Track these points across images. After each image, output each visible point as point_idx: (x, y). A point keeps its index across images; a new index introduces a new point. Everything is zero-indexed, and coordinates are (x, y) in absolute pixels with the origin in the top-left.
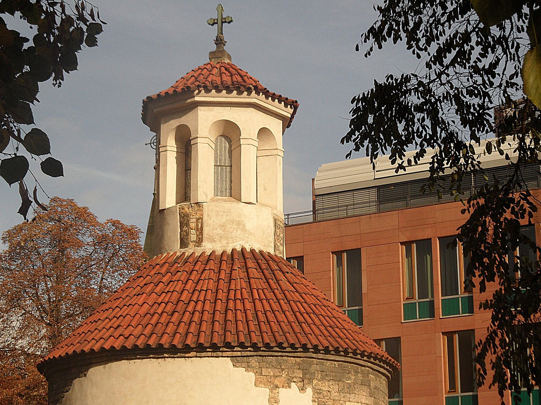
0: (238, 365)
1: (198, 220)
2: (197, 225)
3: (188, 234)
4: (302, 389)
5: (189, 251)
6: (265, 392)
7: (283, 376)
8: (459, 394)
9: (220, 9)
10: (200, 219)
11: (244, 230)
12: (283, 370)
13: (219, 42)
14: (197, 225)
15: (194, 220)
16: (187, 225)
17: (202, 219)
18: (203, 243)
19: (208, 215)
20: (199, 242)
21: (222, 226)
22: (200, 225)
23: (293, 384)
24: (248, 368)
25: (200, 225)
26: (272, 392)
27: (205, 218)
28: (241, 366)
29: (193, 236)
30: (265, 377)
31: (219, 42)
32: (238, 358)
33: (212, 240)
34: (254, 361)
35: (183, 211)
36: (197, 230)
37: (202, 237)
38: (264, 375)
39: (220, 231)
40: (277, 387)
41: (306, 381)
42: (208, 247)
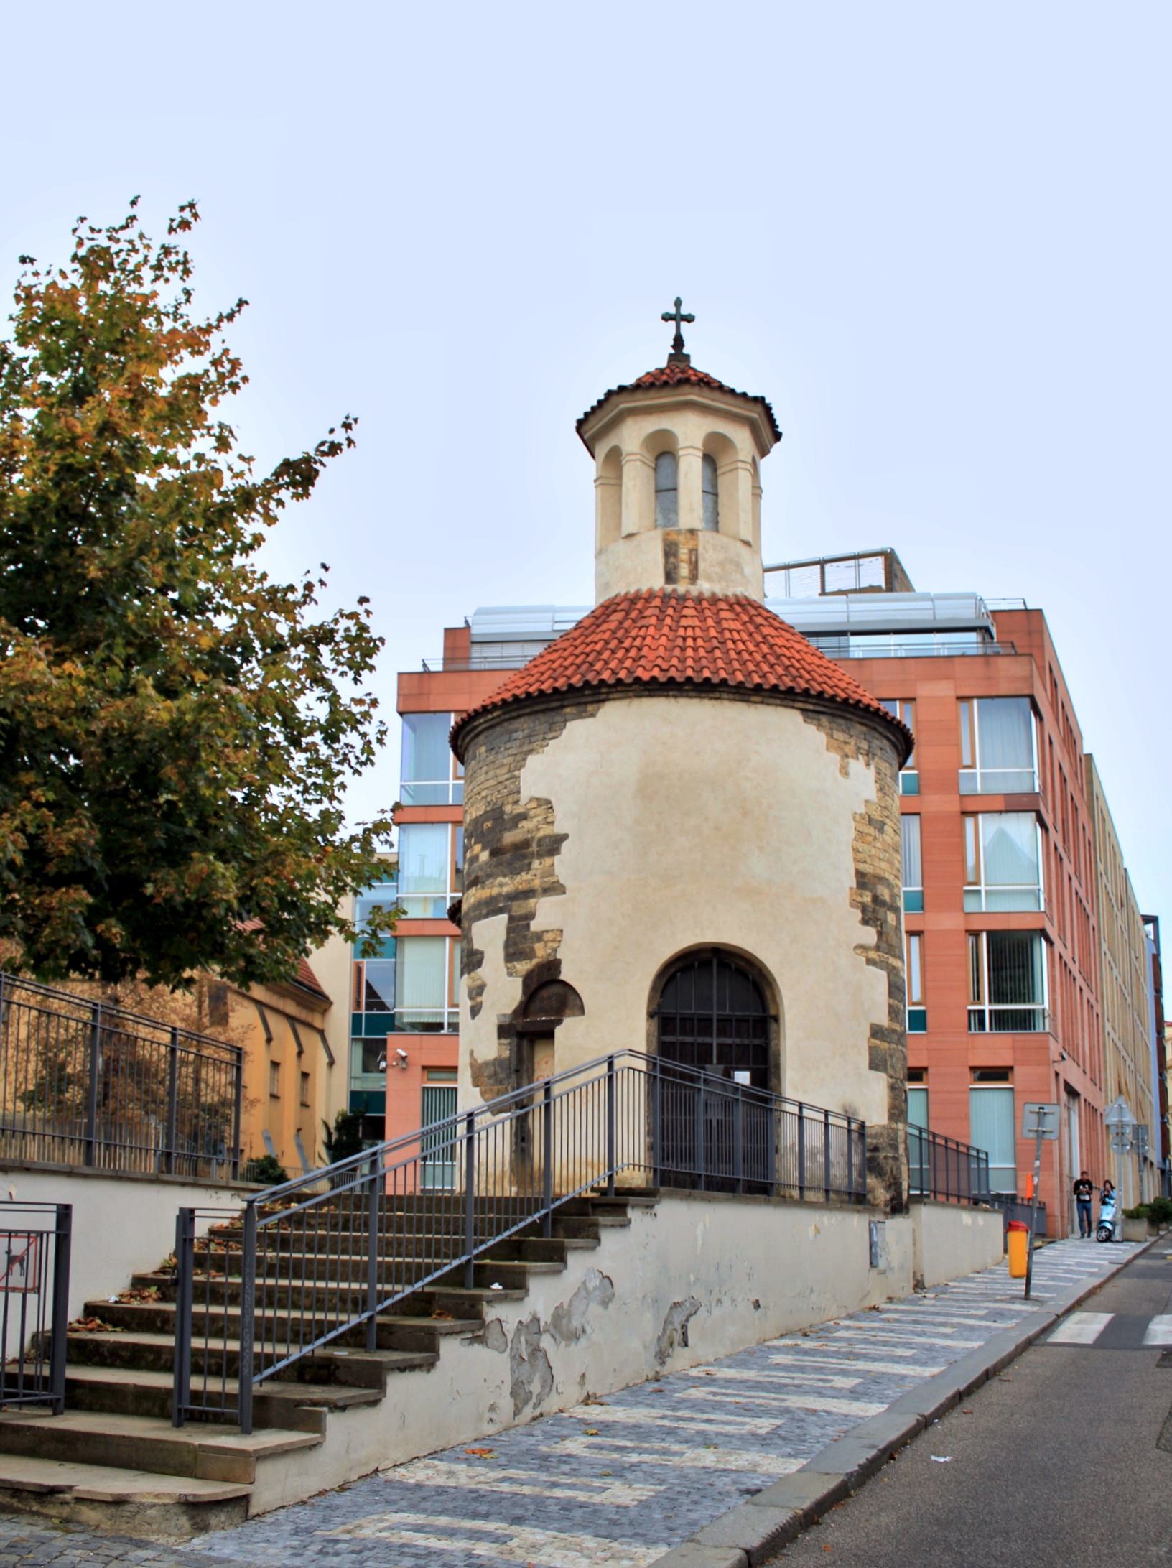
1: (691, 551)
3: (676, 567)
4: (868, 765)
5: (681, 588)
6: (835, 757)
10: (693, 551)
16: (675, 555)
17: (696, 550)
20: (694, 577)
21: (721, 564)
24: (819, 726)
27: (701, 550)
29: (684, 570)
33: (709, 579)
34: (824, 720)
35: (670, 538)
36: (690, 562)
39: (718, 570)
40: (847, 756)
42: (705, 586)
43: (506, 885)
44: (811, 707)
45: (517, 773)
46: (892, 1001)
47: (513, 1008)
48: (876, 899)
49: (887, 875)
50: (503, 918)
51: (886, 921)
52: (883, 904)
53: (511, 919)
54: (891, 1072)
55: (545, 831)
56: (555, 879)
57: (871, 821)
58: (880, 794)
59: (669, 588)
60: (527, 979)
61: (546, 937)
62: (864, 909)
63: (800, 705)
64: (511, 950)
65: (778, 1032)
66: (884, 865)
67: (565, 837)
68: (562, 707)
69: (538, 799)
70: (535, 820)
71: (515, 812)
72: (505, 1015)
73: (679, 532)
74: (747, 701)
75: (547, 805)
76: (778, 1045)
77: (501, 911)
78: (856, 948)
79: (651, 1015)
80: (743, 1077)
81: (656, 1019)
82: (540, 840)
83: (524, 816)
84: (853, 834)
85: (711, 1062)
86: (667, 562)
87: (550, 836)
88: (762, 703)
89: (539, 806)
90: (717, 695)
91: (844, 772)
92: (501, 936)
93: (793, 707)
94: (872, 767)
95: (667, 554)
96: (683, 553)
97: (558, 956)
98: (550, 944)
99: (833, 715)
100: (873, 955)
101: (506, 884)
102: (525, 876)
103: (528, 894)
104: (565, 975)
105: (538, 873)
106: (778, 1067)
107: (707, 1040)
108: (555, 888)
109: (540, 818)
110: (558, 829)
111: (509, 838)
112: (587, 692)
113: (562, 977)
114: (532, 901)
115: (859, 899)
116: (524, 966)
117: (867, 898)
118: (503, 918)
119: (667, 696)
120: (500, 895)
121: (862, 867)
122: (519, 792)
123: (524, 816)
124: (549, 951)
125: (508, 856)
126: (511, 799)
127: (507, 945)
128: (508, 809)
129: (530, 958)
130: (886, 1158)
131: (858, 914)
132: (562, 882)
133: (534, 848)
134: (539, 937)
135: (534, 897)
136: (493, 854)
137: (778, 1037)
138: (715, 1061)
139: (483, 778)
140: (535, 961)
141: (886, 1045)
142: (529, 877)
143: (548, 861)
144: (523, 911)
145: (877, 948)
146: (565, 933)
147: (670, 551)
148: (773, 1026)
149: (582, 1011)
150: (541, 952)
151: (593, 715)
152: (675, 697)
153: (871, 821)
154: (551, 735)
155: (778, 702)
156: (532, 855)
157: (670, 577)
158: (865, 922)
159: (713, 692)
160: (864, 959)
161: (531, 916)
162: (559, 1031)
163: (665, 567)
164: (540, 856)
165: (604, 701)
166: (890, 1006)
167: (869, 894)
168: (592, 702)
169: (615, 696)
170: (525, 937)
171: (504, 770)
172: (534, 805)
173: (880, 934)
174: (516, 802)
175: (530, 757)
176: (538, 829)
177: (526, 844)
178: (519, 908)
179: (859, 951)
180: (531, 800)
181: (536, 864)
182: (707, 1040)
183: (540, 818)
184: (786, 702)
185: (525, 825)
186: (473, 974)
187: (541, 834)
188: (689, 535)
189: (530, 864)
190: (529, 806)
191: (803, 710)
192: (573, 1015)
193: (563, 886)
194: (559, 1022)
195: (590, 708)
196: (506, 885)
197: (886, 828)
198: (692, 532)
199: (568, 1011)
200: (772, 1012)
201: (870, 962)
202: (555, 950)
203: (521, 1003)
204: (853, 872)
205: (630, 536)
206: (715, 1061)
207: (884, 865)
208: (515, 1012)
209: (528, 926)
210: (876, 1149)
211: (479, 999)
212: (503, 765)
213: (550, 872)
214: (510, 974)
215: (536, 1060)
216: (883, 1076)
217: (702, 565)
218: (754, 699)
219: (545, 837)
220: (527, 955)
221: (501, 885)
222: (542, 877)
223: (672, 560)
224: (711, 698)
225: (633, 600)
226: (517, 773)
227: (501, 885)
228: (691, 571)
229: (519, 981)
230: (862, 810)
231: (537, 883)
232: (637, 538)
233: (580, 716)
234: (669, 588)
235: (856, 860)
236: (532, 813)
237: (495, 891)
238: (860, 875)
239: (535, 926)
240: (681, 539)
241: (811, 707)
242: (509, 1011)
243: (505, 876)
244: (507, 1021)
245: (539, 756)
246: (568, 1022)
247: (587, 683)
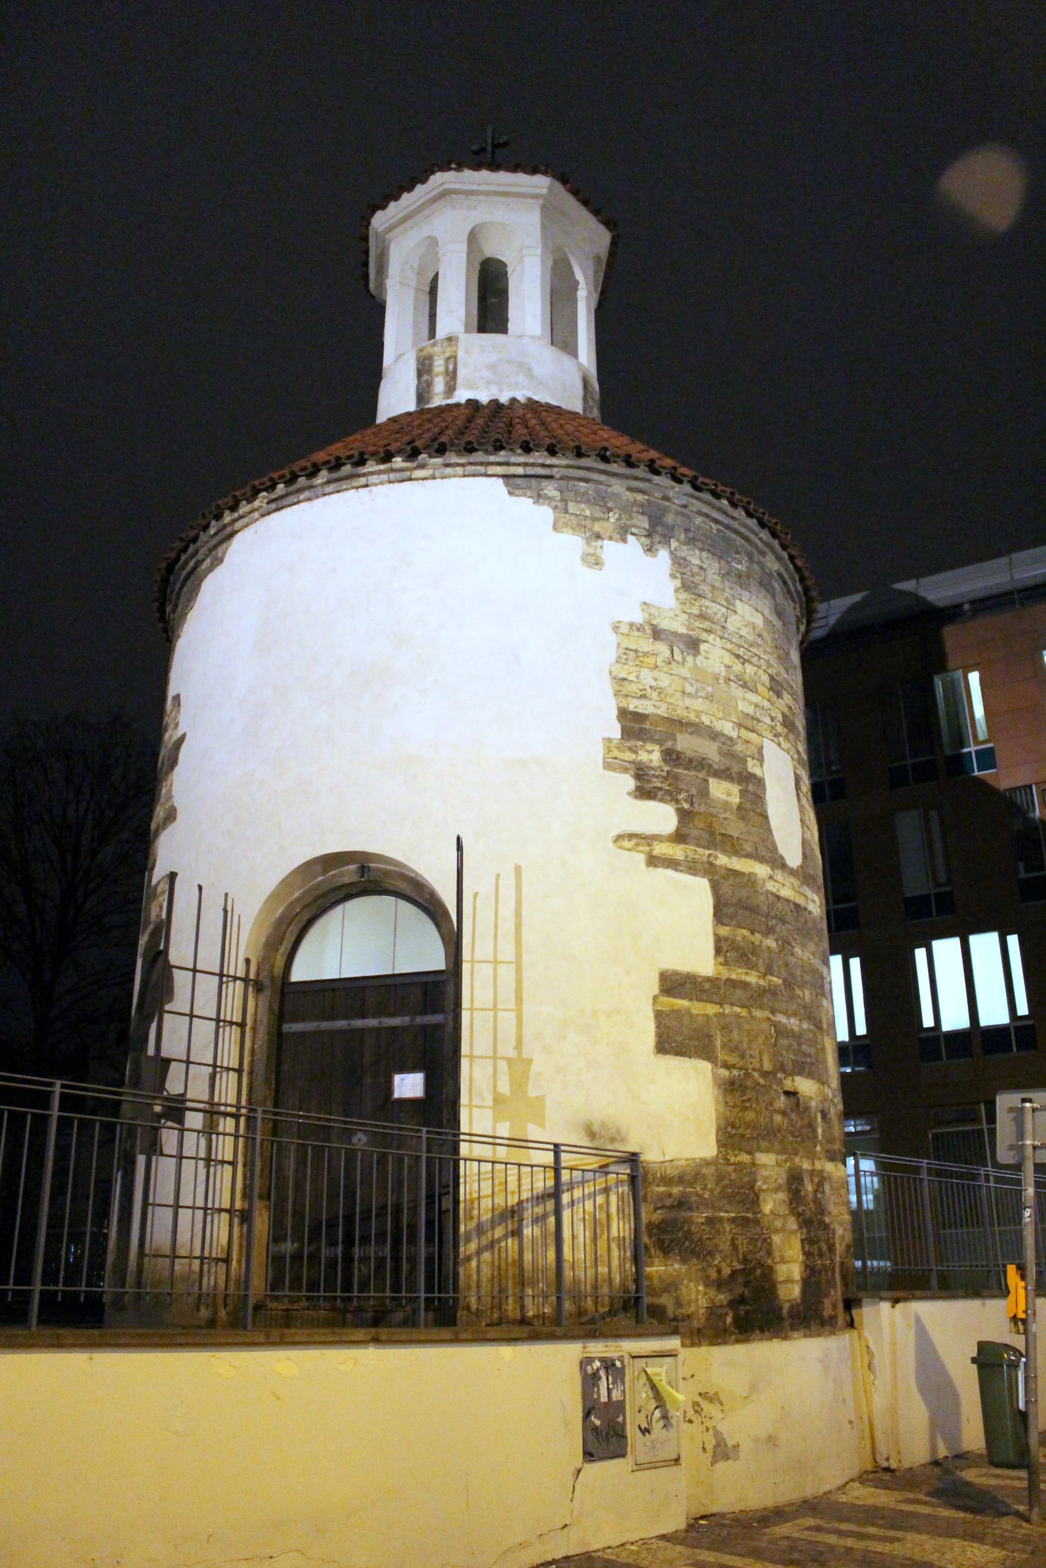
0: (517, 492)
1: (447, 360)
3: (429, 384)
4: (650, 550)
6: (573, 543)
7: (612, 520)
10: (453, 358)
11: (529, 372)
12: (610, 510)
17: (455, 357)
18: (457, 393)
19: (466, 352)
20: (451, 389)
22: (451, 367)
23: (631, 538)
24: (539, 497)
26: (588, 543)
27: (461, 355)
28: (524, 495)
30: (573, 518)
32: (519, 481)
33: (471, 386)
38: (572, 514)
40: (598, 537)
41: (657, 538)
44: (520, 470)
46: (724, 931)
48: (671, 756)
49: (706, 720)
51: (704, 792)
52: (700, 764)
54: (721, 1055)
57: (657, 634)
58: (684, 596)
62: (641, 773)
66: (699, 704)
78: (619, 838)
84: (612, 655)
86: (419, 382)
88: (434, 478)
91: (594, 562)
94: (663, 556)
95: (420, 374)
96: (439, 366)
100: (661, 849)
115: (629, 756)
117: (652, 756)
121: (633, 705)
130: (711, 1221)
131: (629, 782)
141: (711, 1009)
145: (679, 837)
152: (309, 499)
153: (657, 634)
158: (644, 792)
160: (641, 858)
166: (718, 940)
167: (657, 748)
173: (684, 816)
179: (627, 844)
191: (504, 476)
197: (703, 647)
201: (653, 861)
204: (614, 713)
207: (699, 704)
210: (682, 1203)
216: (706, 1066)
217: (461, 373)
223: (425, 377)
230: (638, 618)
235: (617, 694)
238: (624, 714)
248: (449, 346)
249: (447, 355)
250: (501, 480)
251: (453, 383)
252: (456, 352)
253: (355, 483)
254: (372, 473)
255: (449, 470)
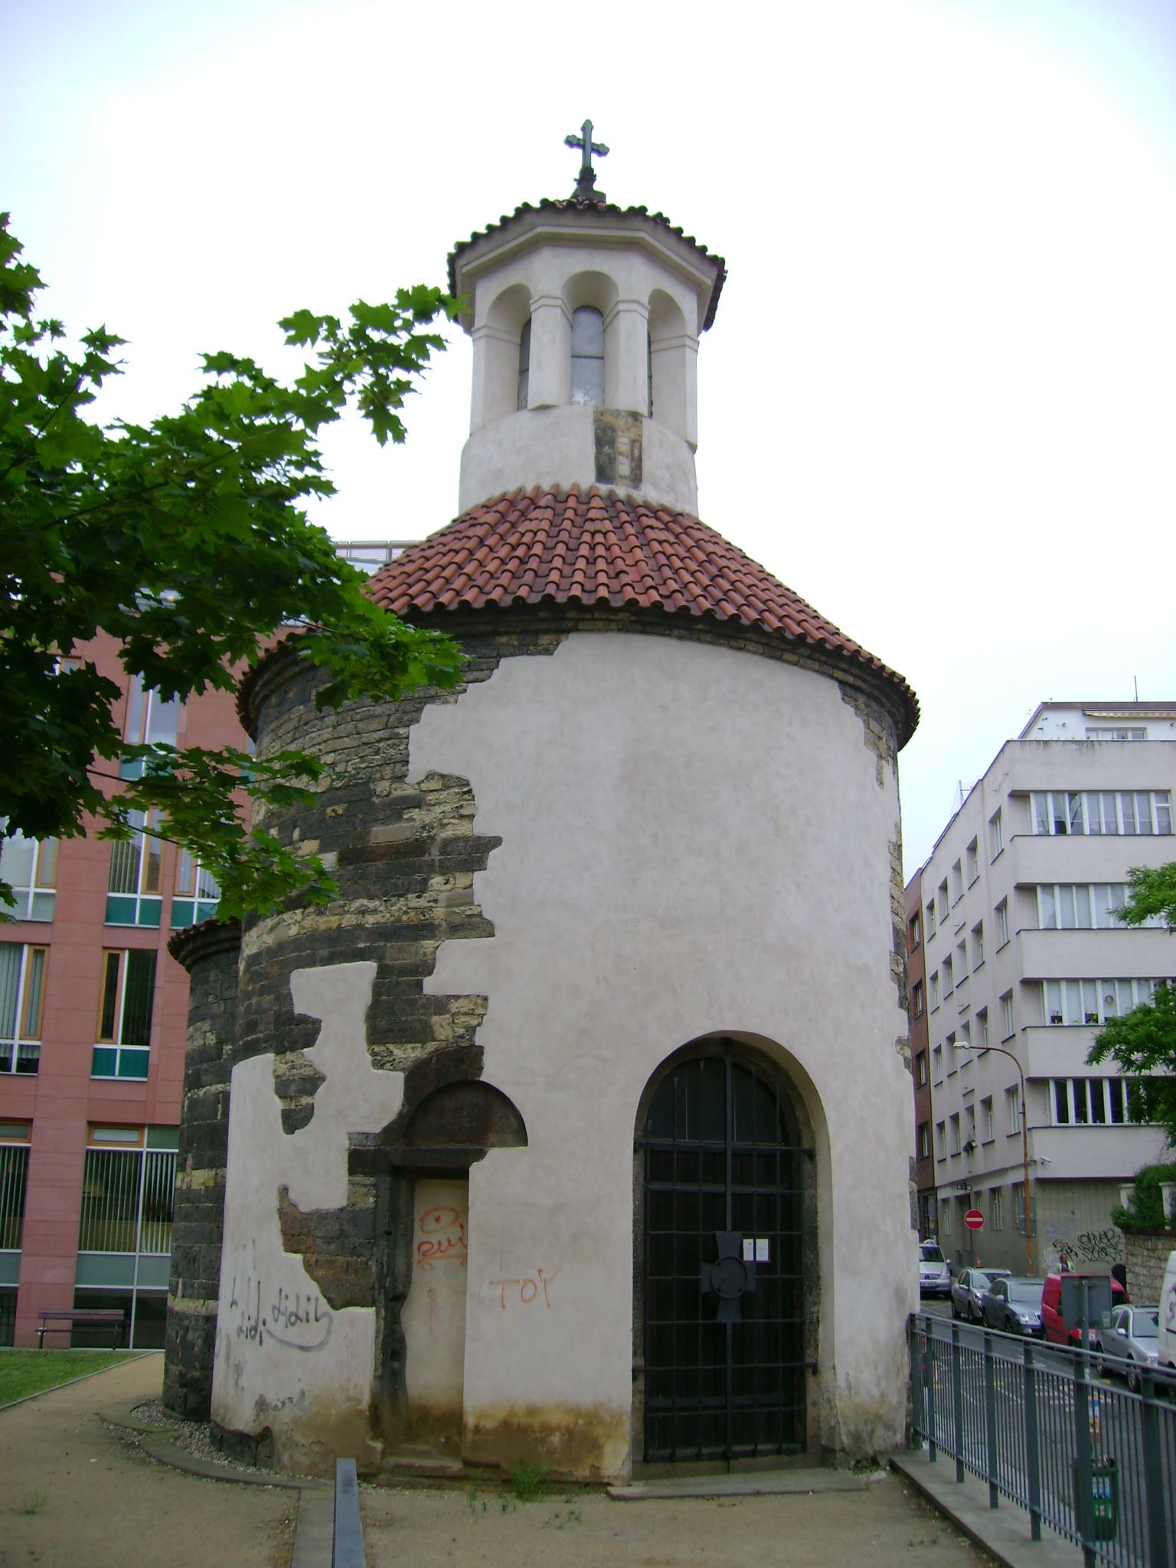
0: (846, 698)
1: (633, 442)
2: (632, 452)
3: (612, 461)
5: (621, 491)
8: (197, 900)
9: (587, 127)
10: (636, 443)
12: (884, 729)
13: (587, 176)
14: (632, 452)
15: (626, 441)
16: (612, 443)
20: (636, 479)
22: (636, 454)
25: (636, 454)
27: (645, 444)
28: (848, 703)
29: (624, 467)
31: (587, 176)
32: (847, 689)
33: (656, 486)
34: (861, 699)
35: (605, 419)
36: (633, 459)
37: (641, 474)
43: (379, 913)
44: (851, 679)
45: (401, 731)
47: (385, 1123)
50: (369, 967)
53: (383, 971)
55: (461, 829)
56: (475, 911)
59: (604, 488)
60: (415, 1076)
61: (454, 1006)
63: (838, 674)
64: (383, 1024)
65: (814, 1176)
67: (496, 842)
68: (497, 633)
69: (443, 776)
70: (438, 809)
71: (395, 794)
72: (367, 1135)
73: (617, 413)
74: (780, 659)
75: (463, 788)
76: (814, 1197)
77: (361, 955)
79: (637, 1147)
80: (758, 1250)
81: (641, 1154)
82: (446, 843)
83: (416, 802)
85: (723, 1228)
87: (466, 839)
88: (796, 664)
89: (446, 787)
90: (741, 643)
92: (364, 996)
93: (831, 677)
96: (623, 443)
97: (478, 1040)
98: (463, 1019)
99: (870, 696)
101: (375, 911)
102: (413, 901)
103: (425, 929)
104: (491, 1074)
105: (442, 897)
106: (814, 1232)
107: (720, 1188)
108: (476, 926)
109: (447, 808)
110: (482, 827)
111: (381, 834)
112: (542, 614)
113: (483, 1078)
114: (428, 944)
116: (409, 1053)
118: (369, 967)
119: (669, 635)
120: (360, 927)
122: (407, 762)
123: (416, 802)
124: (461, 1031)
125: (380, 864)
126: (388, 772)
127: (374, 1014)
128: (382, 787)
129: (423, 1042)
132: (486, 915)
133: (435, 855)
134: (441, 1004)
135: (432, 937)
136: (343, 859)
137: (814, 1185)
138: (729, 1227)
139: (326, 734)
140: (431, 1046)
142: (422, 902)
143: (462, 880)
144: (409, 960)
146: (491, 1003)
147: (604, 438)
148: (807, 1166)
149: (520, 1136)
150: (444, 1029)
151: (548, 652)
152: (681, 638)
154: (471, 676)
155: (817, 666)
156: (431, 868)
157: (604, 472)
159: (736, 638)
161: (428, 968)
162: (476, 1170)
163: (597, 459)
164: (445, 869)
165: (568, 631)
168: (547, 632)
169: (589, 625)
170: (412, 1003)
171: (375, 725)
172: (435, 784)
174: (400, 778)
175: (429, 710)
176: (443, 826)
177: (418, 847)
178: (400, 954)
180: (430, 776)
181: (436, 881)
182: (720, 1188)
183: (447, 808)
184: (825, 668)
185: (415, 813)
186: (289, 1056)
187: (447, 833)
188: (630, 419)
189: (425, 881)
190: (424, 786)
191: (842, 683)
192: (503, 1144)
193: (489, 923)
194: (480, 1155)
195: (544, 640)
196: (379, 913)
198: (635, 416)
199: (492, 1137)
200: (806, 1145)
202: (472, 1030)
203: (400, 1114)
205: (544, 408)
206: (729, 1227)
208: (387, 1130)
209: (420, 984)
211: (305, 1100)
212: (374, 717)
213: (466, 897)
214: (379, 1064)
215: (416, 1207)
217: (647, 465)
218: (787, 656)
219: (456, 839)
220: (423, 1034)
221: (363, 912)
222: (448, 906)
223: (606, 449)
224: (731, 647)
225: (559, 498)
226: (401, 731)
227: (363, 912)
228: (632, 470)
229: (400, 1077)
231: (439, 912)
232: (555, 412)
233: (523, 650)
234: (604, 488)
236: (431, 797)
237: (349, 920)
239: (431, 985)
240: (621, 423)
241: (851, 679)
242: (377, 1129)
243: (371, 898)
244: (370, 1145)
245: (449, 708)
246: (496, 1156)
247: (549, 599)
248: (634, 425)
249: (632, 436)
250: (836, 684)
251: (639, 472)
252: (640, 436)
253: (733, 643)
254: (750, 640)
255: (810, 662)
